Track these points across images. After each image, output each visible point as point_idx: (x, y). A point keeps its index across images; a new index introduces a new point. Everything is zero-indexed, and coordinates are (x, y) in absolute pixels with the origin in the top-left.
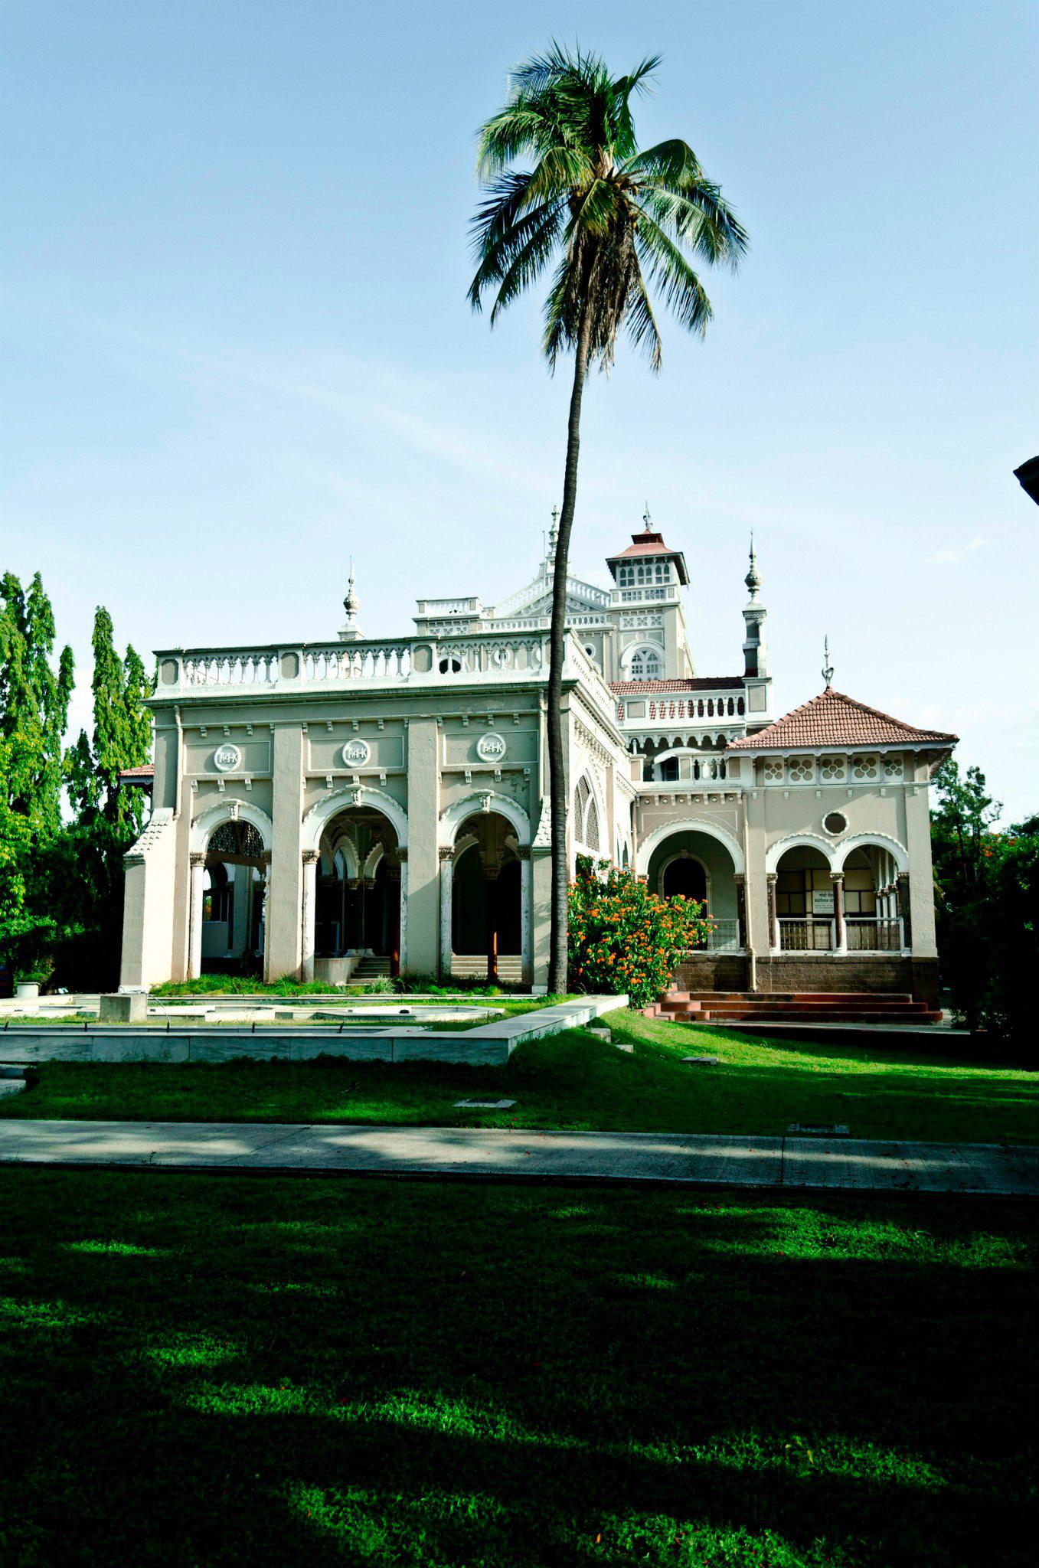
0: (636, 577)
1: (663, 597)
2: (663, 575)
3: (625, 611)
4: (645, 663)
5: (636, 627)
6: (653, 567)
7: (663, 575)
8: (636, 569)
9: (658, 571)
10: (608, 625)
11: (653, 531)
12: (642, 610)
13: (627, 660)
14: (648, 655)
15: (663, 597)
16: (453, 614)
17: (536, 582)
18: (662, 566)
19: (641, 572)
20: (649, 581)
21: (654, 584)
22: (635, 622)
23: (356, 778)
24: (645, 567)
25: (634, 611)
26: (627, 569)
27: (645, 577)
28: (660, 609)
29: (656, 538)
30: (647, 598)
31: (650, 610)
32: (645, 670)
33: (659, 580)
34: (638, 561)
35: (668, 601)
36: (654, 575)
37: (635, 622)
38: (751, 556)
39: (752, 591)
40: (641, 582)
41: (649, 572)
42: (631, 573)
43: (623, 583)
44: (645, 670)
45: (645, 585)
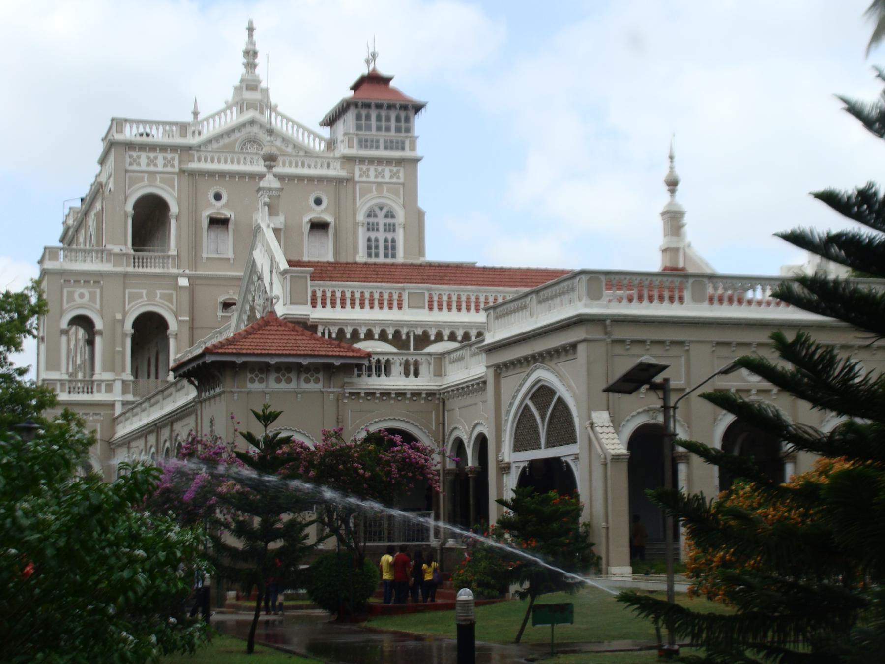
1: (403, 148)
2: (403, 124)
3: (362, 160)
4: (381, 220)
5: (372, 179)
6: (393, 115)
7: (403, 124)
8: (373, 114)
9: (398, 119)
10: (343, 173)
11: (383, 71)
12: (380, 161)
13: (361, 217)
14: (384, 211)
15: (403, 148)
16: (144, 139)
17: (229, 107)
18: (403, 114)
19: (379, 119)
21: (393, 133)
22: (372, 173)
23: (754, 392)
24: (383, 113)
25: (371, 161)
26: (364, 112)
27: (383, 124)
28: (400, 162)
29: (386, 81)
30: (386, 148)
31: (389, 161)
32: (381, 227)
33: (398, 130)
34: (379, 106)
35: (407, 154)
36: (393, 124)
37: (372, 173)
38: (671, 158)
40: (379, 129)
41: (388, 119)
42: (368, 117)
43: (359, 128)
44: (381, 227)
45: (383, 133)
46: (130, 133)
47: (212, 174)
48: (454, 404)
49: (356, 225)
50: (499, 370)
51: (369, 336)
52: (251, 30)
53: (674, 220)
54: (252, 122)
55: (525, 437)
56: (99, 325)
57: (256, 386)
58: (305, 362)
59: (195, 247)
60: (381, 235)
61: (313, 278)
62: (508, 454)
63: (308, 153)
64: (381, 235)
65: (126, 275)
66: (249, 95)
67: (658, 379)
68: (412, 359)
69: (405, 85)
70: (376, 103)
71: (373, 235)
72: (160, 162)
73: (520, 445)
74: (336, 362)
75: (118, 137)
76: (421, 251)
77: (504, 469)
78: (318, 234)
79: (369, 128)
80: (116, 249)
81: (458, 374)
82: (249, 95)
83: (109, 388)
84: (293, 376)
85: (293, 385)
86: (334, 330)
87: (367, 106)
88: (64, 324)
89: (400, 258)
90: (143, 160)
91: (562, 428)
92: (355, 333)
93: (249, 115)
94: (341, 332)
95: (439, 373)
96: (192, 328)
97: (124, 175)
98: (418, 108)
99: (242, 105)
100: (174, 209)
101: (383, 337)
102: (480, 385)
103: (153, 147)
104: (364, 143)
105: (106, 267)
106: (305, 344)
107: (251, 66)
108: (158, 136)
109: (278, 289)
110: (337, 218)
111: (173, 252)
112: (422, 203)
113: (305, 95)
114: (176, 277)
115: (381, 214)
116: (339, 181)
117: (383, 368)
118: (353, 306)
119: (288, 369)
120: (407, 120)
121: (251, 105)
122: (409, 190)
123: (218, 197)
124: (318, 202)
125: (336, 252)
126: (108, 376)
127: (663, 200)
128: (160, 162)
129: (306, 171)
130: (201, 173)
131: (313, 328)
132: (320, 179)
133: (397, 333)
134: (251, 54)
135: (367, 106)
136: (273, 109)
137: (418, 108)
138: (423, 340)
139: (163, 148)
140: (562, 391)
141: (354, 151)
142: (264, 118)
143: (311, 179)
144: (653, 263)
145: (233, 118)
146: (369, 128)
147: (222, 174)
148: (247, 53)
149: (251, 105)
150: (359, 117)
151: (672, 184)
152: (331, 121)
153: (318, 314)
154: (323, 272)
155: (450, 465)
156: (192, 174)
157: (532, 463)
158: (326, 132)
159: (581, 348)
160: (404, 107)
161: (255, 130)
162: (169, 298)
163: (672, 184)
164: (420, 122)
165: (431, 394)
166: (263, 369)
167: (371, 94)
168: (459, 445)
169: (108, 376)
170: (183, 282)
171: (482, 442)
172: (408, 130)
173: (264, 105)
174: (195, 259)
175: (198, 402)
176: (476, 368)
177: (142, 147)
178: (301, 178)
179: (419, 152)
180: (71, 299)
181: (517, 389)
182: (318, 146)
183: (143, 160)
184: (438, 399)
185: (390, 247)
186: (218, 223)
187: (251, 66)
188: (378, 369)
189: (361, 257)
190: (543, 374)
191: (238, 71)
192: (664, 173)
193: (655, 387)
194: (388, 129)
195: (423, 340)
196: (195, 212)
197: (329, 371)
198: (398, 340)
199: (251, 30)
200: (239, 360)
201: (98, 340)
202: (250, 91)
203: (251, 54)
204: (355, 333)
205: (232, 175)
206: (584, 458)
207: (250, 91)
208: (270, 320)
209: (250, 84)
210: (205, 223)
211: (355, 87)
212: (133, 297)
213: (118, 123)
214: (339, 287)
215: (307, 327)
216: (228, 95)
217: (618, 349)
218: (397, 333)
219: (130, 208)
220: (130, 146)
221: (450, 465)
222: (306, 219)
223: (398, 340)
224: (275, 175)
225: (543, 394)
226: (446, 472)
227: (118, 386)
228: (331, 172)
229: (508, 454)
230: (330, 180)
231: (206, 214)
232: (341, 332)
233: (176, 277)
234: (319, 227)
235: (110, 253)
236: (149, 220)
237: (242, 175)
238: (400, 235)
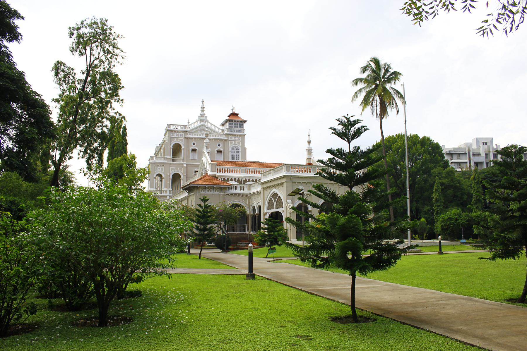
0: (234, 125)
3: (231, 135)
4: (235, 150)
6: (239, 123)
8: (234, 123)
9: (240, 125)
10: (226, 138)
11: (236, 112)
12: (235, 135)
13: (230, 150)
19: (235, 124)
20: (237, 127)
25: (233, 135)
28: (240, 135)
29: (237, 115)
31: (237, 135)
33: (240, 127)
34: (235, 121)
35: (242, 133)
36: (239, 126)
39: (309, 144)
41: (237, 125)
42: (232, 124)
43: (230, 127)
46: (172, 128)
47: (192, 138)
48: (253, 197)
49: (229, 151)
50: (264, 189)
51: (231, 180)
52: (203, 102)
53: (310, 151)
54: (203, 125)
55: (270, 206)
56: (163, 176)
57: (203, 192)
58: (215, 186)
59: (188, 157)
60: (235, 154)
61: (217, 165)
62: (266, 210)
63: (217, 133)
64: (235, 154)
65: (170, 164)
66: (202, 118)
67: (301, 192)
68: (242, 186)
69: (242, 116)
70: (234, 120)
71: (233, 154)
72: (179, 135)
73: (268, 209)
74: (223, 186)
75: (169, 129)
76: (245, 158)
77: (265, 214)
78: (219, 154)
79: (232, 127)
80: (169, 157)
81: (254, 190)
82: (202, 118)
83: (166, 192)
84: (212, 190)
85: (212, 192)
86: (223, 178)
87: (232, 121)
88: (155, 176)
89: (240, 160)
90: (175, 135)
91: (280, 204)
92: (228, 179)
93: (202, 123)
94: (224, 179)
95: (249, 190)
96: (187, 177)
97: (170, 138)
98: (245, 122)
99: (200, 121)
100: (183, 147)
101: (235, 180)
102: (259, 193)
103: (178, 131)
104: (231, 131)
105: (166, 162)
106: (215, 182)
107: (203, 111)
108: (179, 128)
109: (208, 168)
110: (224, 150)
111: (182, 158)
112: (246, 146)
113: (217, 118)
114: (183, 164)
115: (235, 149)
116: (225, 140)
117: (235, 188)
118: (227, 172)
119: (212, 188)
120: (242, 125)
121: (203, 121)
122: (243, 143)
123: (194, 144)
124: (219, 145)
125: (224, 159)
126: (165, 189)
127: (307, 146)
128: (179, 135)
129: (216, 138)
130: (190, 138)
131: (217, 178)
132: (220, 140)
133: (239, 179)
134: (203, 108)
135: (232, 121)
136: (208, 122)
137: (245, 122)
138: (245, 181)
139: (180, 131)
140: (280, 194)
141: (228, 133)
142: (206, 124)
143: (217, 139)
144: (304, 162)
145: (198, 124)
146: (232, 127)
147: (195, 138)
148: (202, 107)
149: (203, 121)
150: (230, 124)
151: (309, 142)
152: (223, 125)
153: (218, 174)
154: (220, 163)
155: (252, 213)
156: (187, 138)
157: (272, 213)
158: (221, 128)
159: (285, 184)
160: (242, 122)
161: (204, 127)
162: (181, 169)
163: (309, 142)
164: (245, 125)
165: (247, 195)
166: (205, 188)
167: (233, 118)
168: (254, 208)
169: (165, 189)
170: (185, 165)
171: (260, 207)
172: (242, 127)
173: (206, 121)
174: (188, 160)
175: (188, 196)
176: (258, 189)
177: (175, 131)
178: (215, 139)
179: (245, 133)
180: (157, 170)
181: (269, 194)
182: (220, 131)
183: (175, 135)
184: (249, 197)
185: (238, 157)
186: (194, 151)
187: (203, 111)
188: (233, 188)
189: (230, 160)
190: (275, 190)
191: (199, 112)
192: (307, 139)
193: (300, 194)
194: (237, 127)
195: (245, 181)
196: (188, 148)
197: (221, 189)
198: (239, 181)
199: (203, 102)
200: (198, 186)
201: (163, 180)
202: (203, 117)
203: (203, 108)
204: (228, 179)
205: (198, 138)
206: (285, 211)
207: (203, 117)
208: (206, 176)
209: (203, 116)
210: (191, 151)
211: (229, 116)
212: (172, 169)
213: (169, 125)
214: (224, 167)
215: (216, 177)
216: (197, 118)
217: (294, 184)
218: (239, 179)
219: (171, 147)
220: (172, 131)
221: (252, 213)
222: (216, 150)
223: (239, 181)
224: (210, 139)
225: (275, 195)
226: (251, 215)
227: (168, 192)
228: (223, 138)
229: (266, 210)
230: (222, 140)
231: (191, 148)
232: (224, 179)
233: (183, 164)
234: (219, 152)
235: (166, 158)
236: (176, 150)
237: (200, 138)
238: (240, 154)
